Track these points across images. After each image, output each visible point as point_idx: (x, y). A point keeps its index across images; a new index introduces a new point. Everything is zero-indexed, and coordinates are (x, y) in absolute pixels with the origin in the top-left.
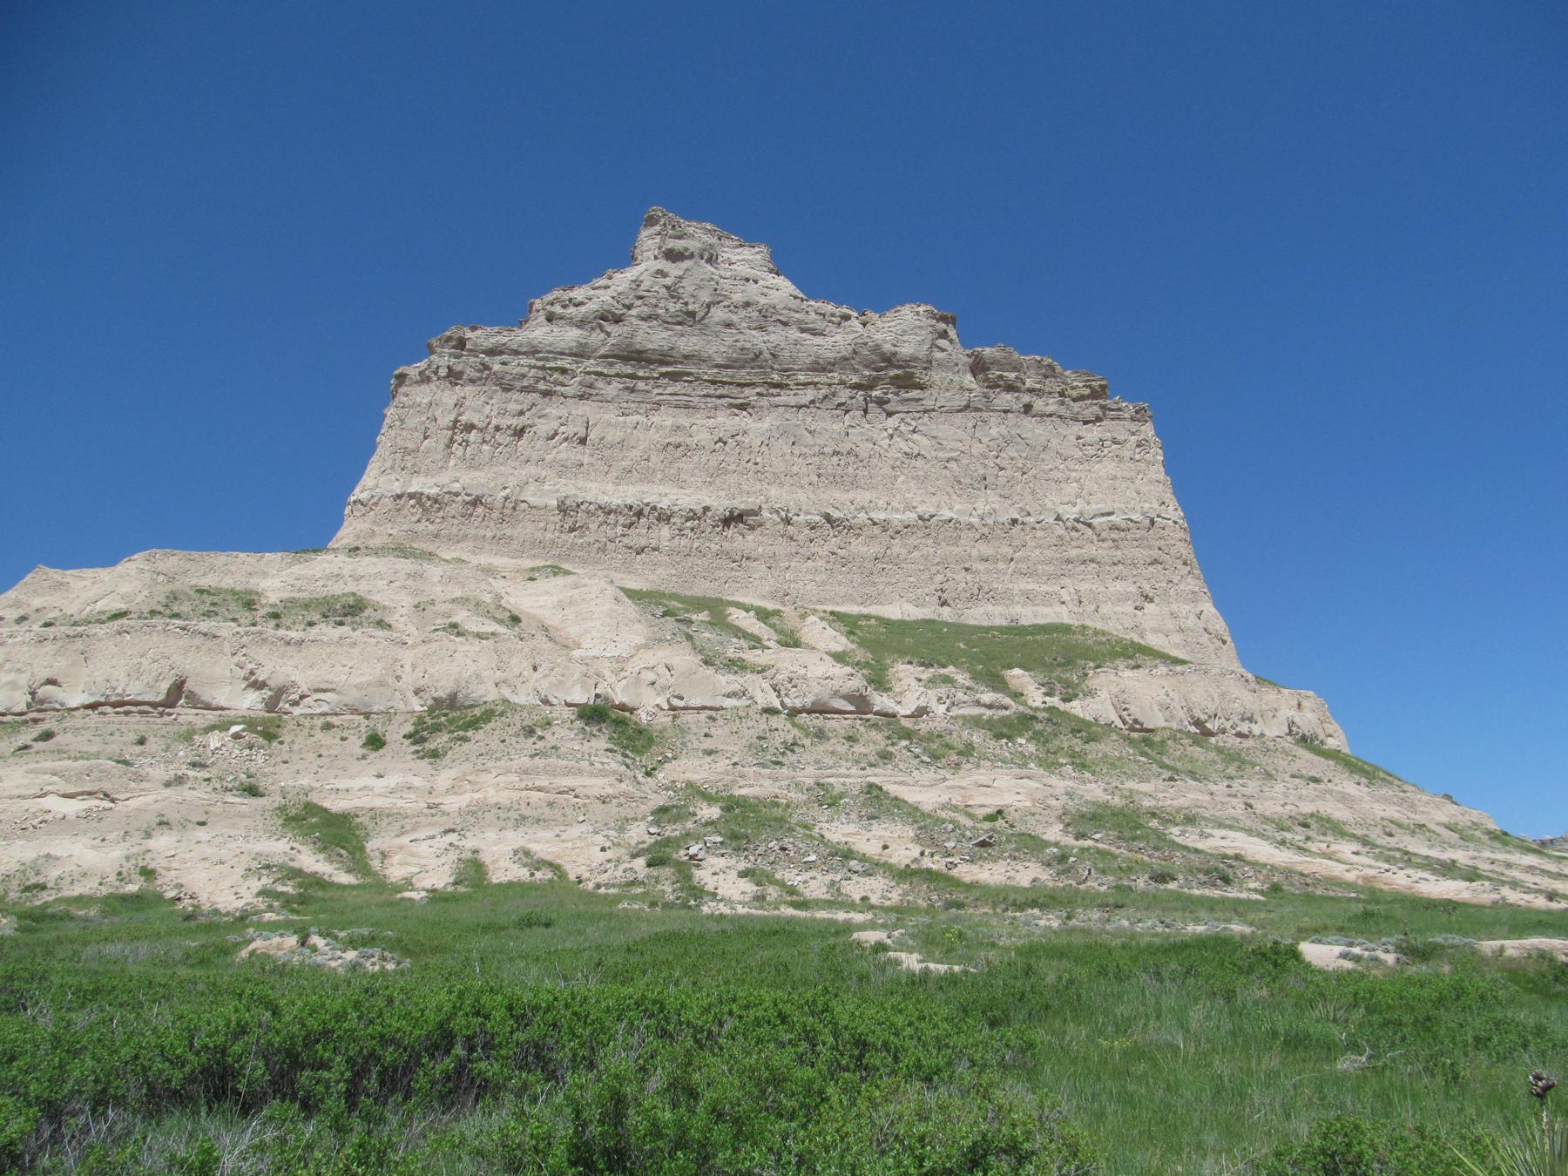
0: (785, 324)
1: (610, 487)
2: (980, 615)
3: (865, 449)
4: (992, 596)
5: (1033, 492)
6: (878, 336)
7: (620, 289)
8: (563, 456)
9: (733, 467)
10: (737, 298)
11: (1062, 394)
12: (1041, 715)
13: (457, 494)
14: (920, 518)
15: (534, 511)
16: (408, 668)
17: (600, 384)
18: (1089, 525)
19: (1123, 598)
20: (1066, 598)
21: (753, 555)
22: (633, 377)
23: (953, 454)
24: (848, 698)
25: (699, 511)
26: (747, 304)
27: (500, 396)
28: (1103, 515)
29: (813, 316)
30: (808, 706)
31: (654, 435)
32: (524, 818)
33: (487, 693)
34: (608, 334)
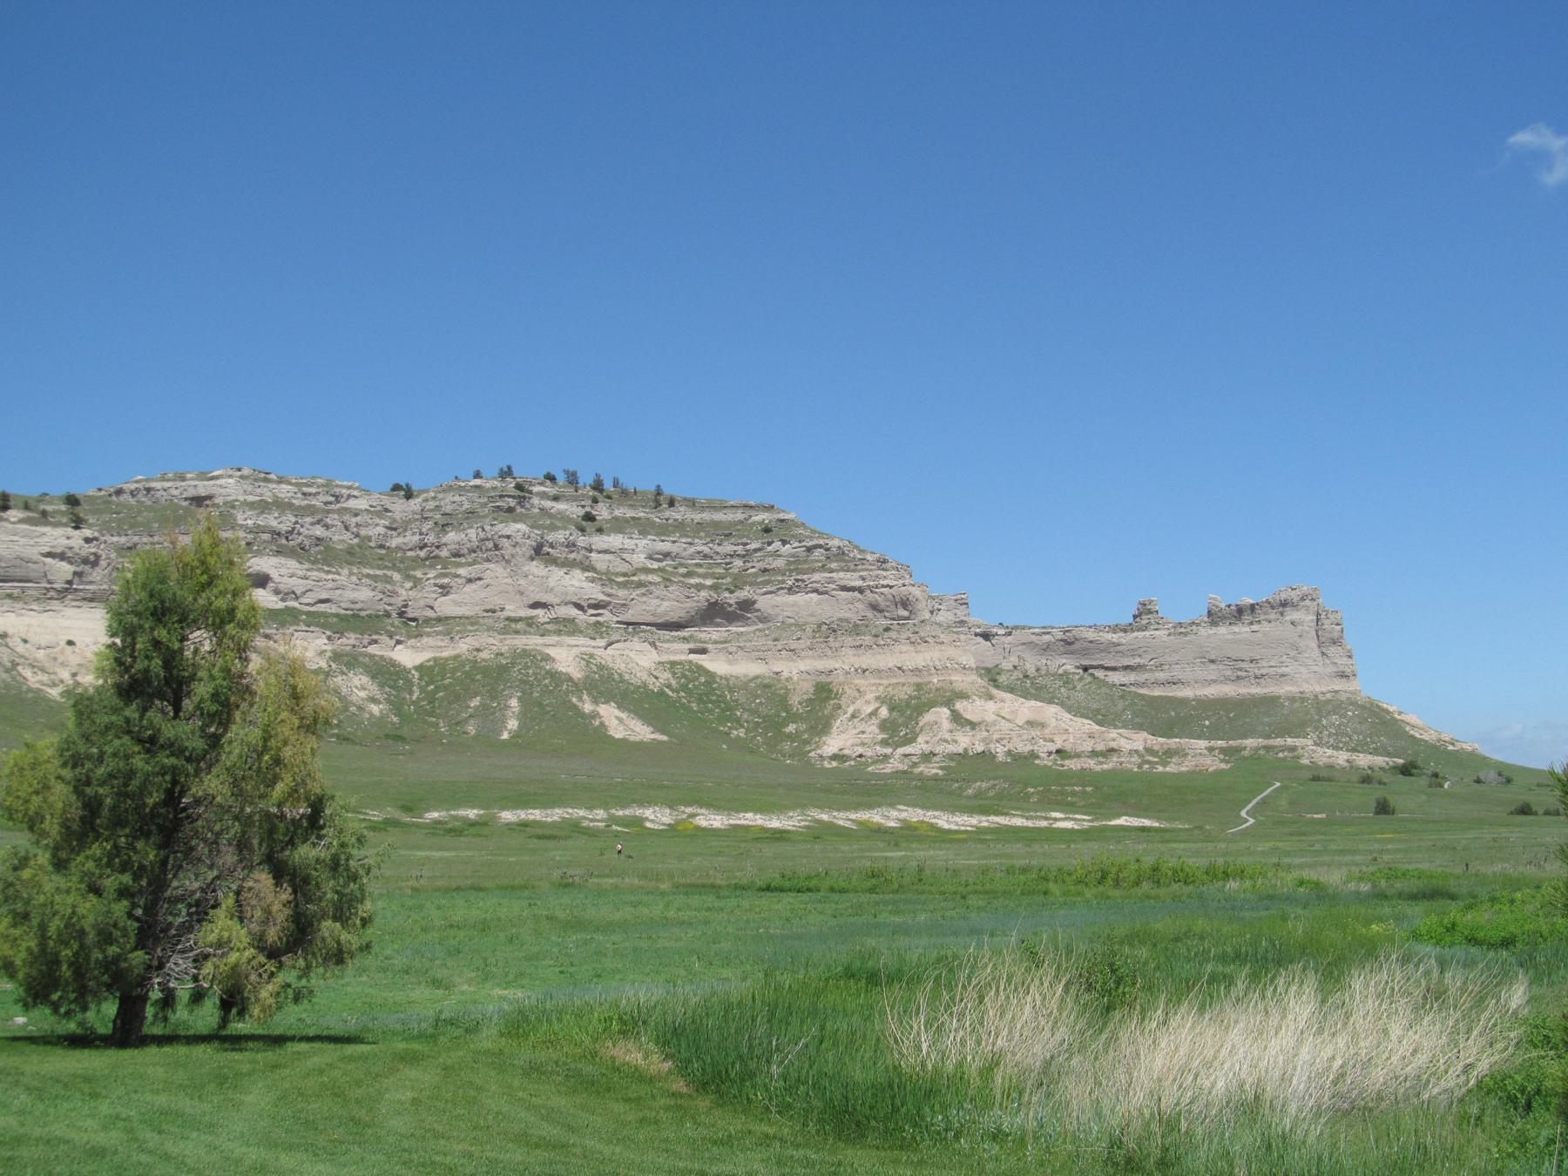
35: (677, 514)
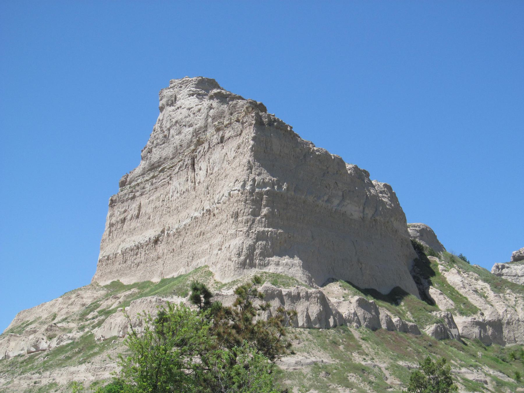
0: (185, 126)
10: (174, 120)
22: (153, 177)
24: (33, 346)
26: (176, 122)
29: (192, 115)
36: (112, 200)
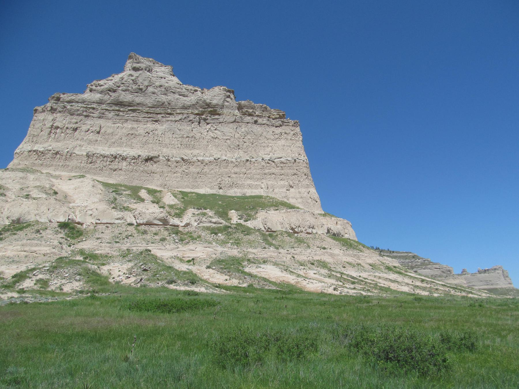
0: (174, 93)
1: (106, 148)
2: (233, 192)
3: (198, 136)
4: (237, 186)
5: (255, 151)
6: (205, 97)
7: (116, 81)
8: (91, 138)
9: (151, 142)
10: (157, 84)
11: (269, 117)
12: (233, 226)
13: (50, 151)
14: (215, 159)
15: (78, 157)
16: (6, 209)
17: (107, 113)
18: (274, 162)
19: (283, 187)
20: (263, 186)
21: (155, 172)
22: (119, 111)
23: (229, 138)
24: (160, 220)
25: (137, 157)
26: (161, 86)
27: (69, 117)
28: (278, 158)
30: (145, 223)
31: (124, 131)
32: (13, 261)
33: (32, 218)
34: (111, 96)
35: (395, 254)
36: (51, 107)
